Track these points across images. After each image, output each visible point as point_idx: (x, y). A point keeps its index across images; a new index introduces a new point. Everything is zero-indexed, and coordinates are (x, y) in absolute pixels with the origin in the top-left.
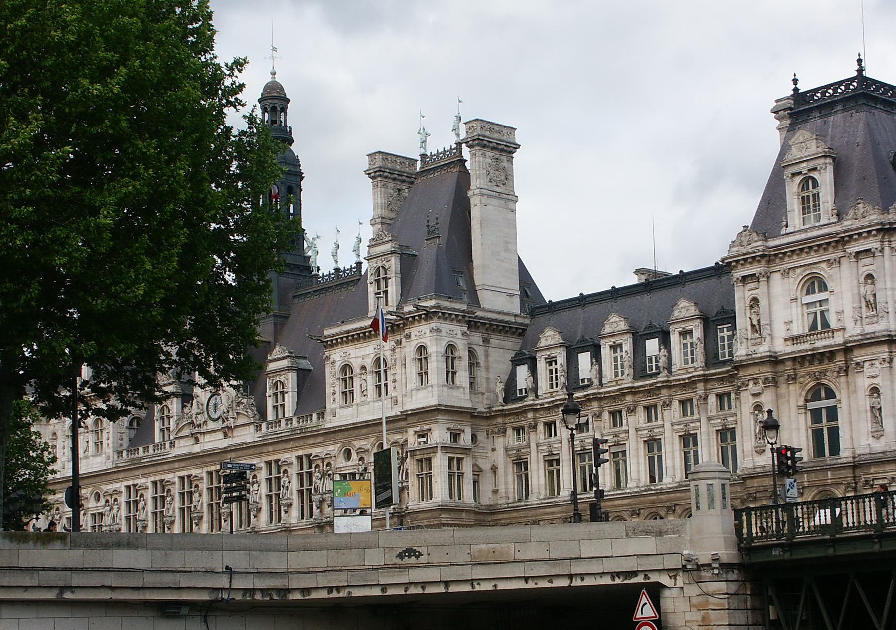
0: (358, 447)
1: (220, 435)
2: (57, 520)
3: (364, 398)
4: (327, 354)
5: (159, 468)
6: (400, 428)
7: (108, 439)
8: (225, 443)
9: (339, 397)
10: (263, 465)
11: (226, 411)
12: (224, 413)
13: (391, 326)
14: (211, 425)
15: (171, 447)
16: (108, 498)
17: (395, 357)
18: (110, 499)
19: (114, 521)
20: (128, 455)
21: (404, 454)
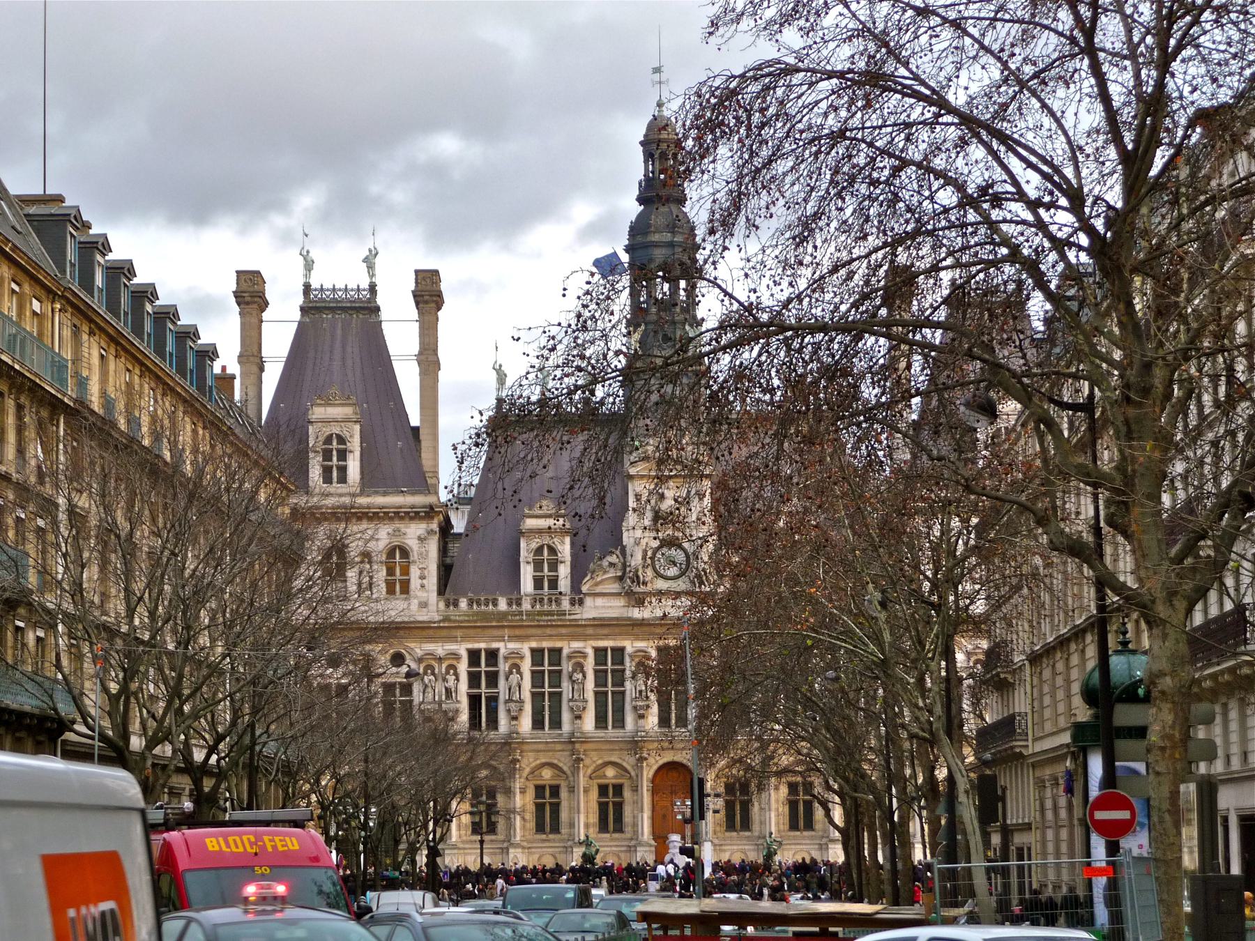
0: (970, 647)
5: (548, 631)
15: (572, 603)
16: (433, 663)
18: (436, 665)
20: (470, 604)
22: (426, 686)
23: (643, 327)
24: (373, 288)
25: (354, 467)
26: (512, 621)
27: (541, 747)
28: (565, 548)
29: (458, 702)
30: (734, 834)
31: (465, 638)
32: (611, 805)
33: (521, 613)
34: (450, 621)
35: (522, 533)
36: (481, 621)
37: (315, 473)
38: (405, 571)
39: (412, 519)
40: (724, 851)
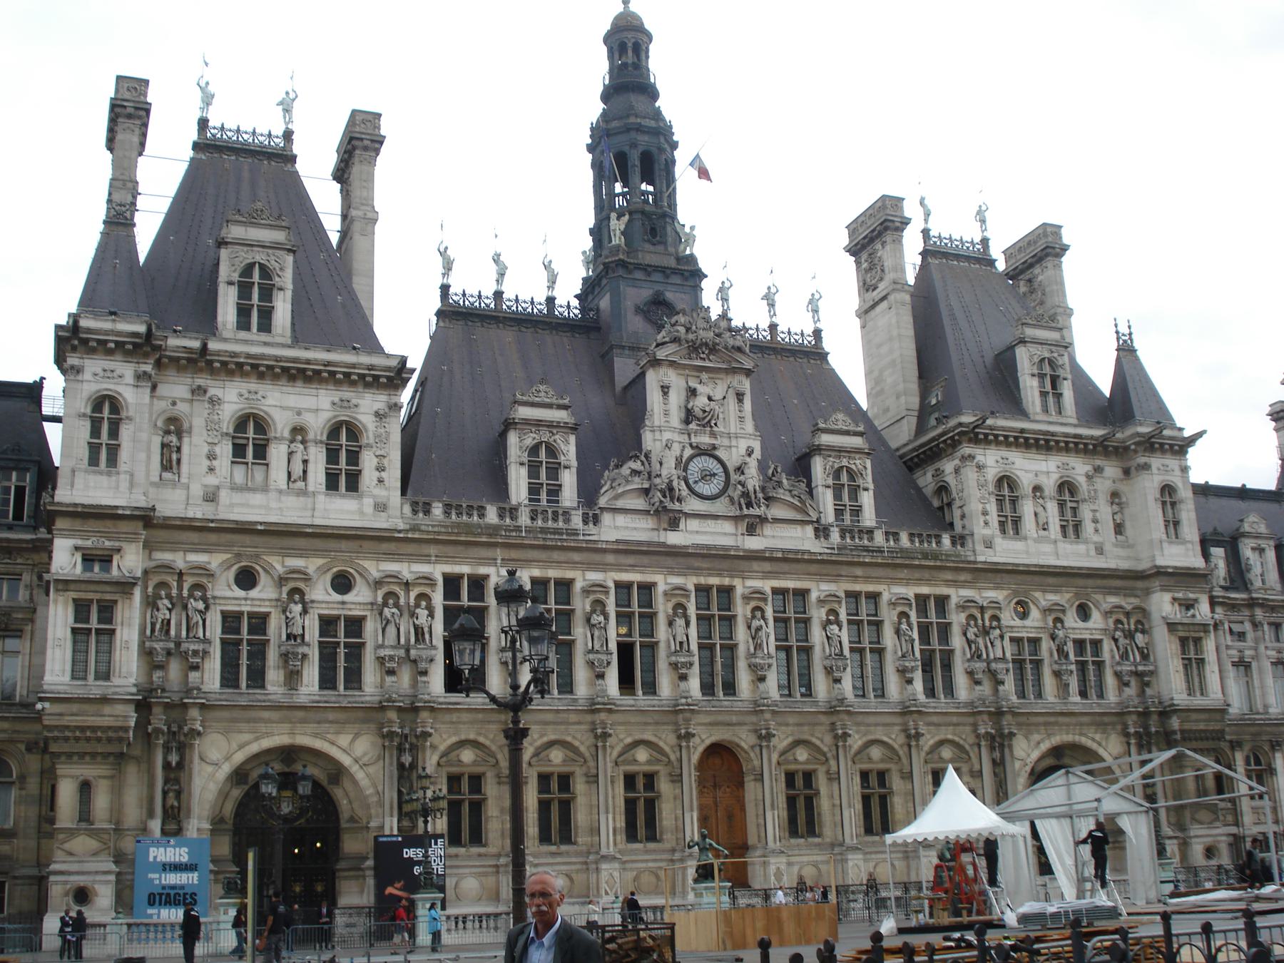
1: (728, 527)
2: (200, 612)
3: (1042, 533)
5: (556, 555)
6: (1116, 588)
8: (753, 543)
9: (994, 518)
10: (843, 595)
11: (757, 488)
13: (1094, 445)
14: (694, 505)
15: (585, 522)
16: (397, 589)
18: (402, 594)
19: (417, 640)
20: (447, 514)
21: (1133, 627)
22: (388, 622)
23: (627, 217)
24: (288, 135)
27: (549, 717)
28: (569, 449)
29: (433, 647)
30: (802, 841)
31: (440, 559)
33: (518, 529)
34: (420, 530)
36: (467, 534)
38: (354, 457)
39: (367, 385)
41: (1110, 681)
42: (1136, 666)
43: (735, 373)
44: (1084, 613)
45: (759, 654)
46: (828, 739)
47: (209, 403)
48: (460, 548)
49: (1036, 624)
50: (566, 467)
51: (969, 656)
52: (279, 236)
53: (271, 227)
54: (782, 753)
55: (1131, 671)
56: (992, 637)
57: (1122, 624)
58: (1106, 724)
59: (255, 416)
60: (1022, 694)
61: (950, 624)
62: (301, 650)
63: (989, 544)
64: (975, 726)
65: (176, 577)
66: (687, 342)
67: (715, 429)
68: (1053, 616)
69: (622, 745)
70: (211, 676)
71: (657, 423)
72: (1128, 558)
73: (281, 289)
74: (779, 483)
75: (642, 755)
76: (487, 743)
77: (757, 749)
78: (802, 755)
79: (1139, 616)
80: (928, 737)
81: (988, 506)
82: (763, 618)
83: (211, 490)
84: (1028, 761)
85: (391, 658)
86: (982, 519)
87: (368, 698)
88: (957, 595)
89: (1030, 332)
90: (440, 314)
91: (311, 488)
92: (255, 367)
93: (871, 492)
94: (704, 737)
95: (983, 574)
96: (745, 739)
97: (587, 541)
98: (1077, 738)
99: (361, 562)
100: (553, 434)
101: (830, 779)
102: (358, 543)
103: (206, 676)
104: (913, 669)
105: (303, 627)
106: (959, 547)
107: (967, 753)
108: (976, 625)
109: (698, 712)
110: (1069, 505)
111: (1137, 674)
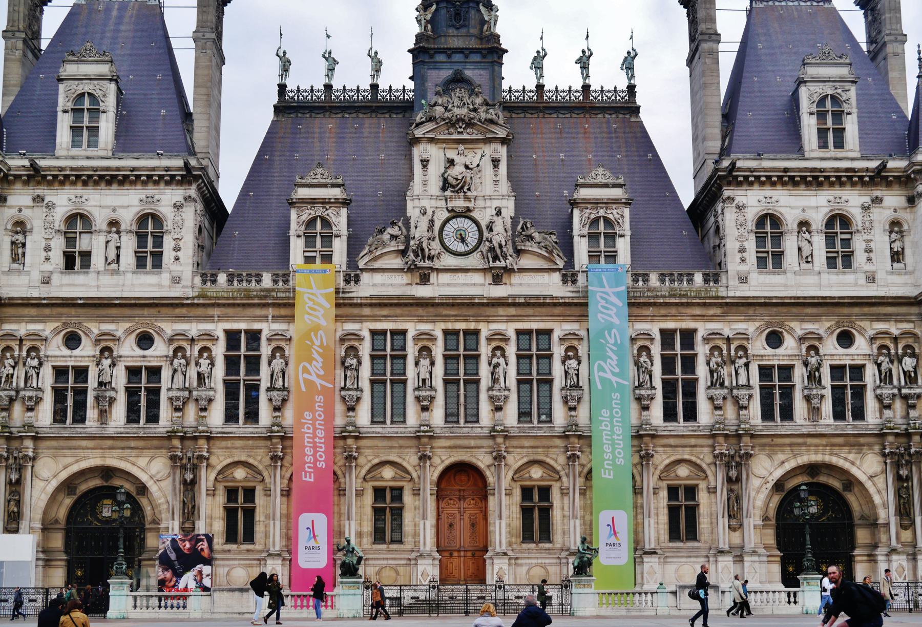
0: (800, 332)
1: (478, 278)
2: (34, 368)
3: (804, 266)
4: (727, 193)
6: (885, 315)
7: (177, 249)
8: (499, 292)
11: (504, 243)
12: (500, 246)
14: (448, 261)
15: (347, 280)
16: (185, 344)
17: (869, 218)
18: (188, 348)
20: (230, 281)
21: (900, 352)
22: (175, 371)
25: (107, 127)
26: (277, 298)
28: (340, 220)
30: (533, 546)
32: (388, 509)
35: (292, 204)
37: (63, 135)
38: (159, 242)
39: (168, 183)
40: (521, 565)
41: (871, 404)
42: (900, 390)
43: (490, 142)
44: (846, 339)
45: (497, 387)
46: (562, 459)
47: (46, 207)
48: (239, 309)
49: (790, 352)
50: (336, 236)
51: (709, 384)
52: (104, 69)
53: (97, 62)
54: (516, 472)
55: (894, 395)
56: (737, 365)
57: (888, 349)
58: (863, 445)
59: (82, 216)
60: (767, 414)
61: (696, 355)
62: (108, 394)
63: (744, 280)
64: (713, 447)
65: (18, 343)
66: (444, 120)
67: (469, 193)
68: (807, 344)
69: (370, 465)
70: (45, 415)
71: (416, 193)
72: (906, 284)
73: (104, 112)
74: (530, 238)
75: (388, 473)
76: (255, 463)
77: (492, 468)
78: (536, 473)
79: (910, 341)
80: (664, 457)
81: (746, 245)
82: (503, 355)
83: (47, 275)
84: (770, 479)
85: (178, 398)
86: (740, 255)
87: (161, 430)
88: (702, 329)
89: (812, 71)
90: (276, 108)
91: (121, 269)
92: (78, 177)
93: (628, 238)
94: (444, 458)
95: (734, 309)
96: (483, 460)
97: (344, 298)
98: (827, 459)
99: (159, 324)
100: (327, 210)
101: (562, 494)
102: (157, 309)
103: (40, 415)
104: (652, 399)
105: (112, 376)
106: (711, 284)
107: (704, 472)
108: (721, 354)
109: (439, 438)
110: (840, 236)
111: (905, 398)
